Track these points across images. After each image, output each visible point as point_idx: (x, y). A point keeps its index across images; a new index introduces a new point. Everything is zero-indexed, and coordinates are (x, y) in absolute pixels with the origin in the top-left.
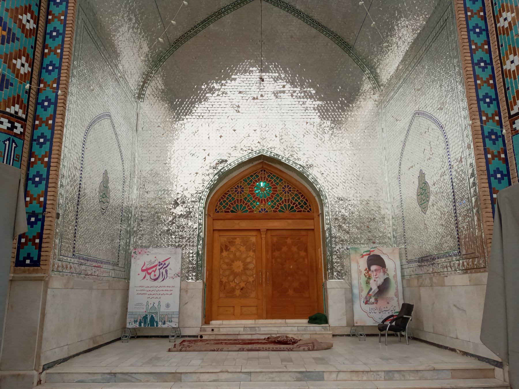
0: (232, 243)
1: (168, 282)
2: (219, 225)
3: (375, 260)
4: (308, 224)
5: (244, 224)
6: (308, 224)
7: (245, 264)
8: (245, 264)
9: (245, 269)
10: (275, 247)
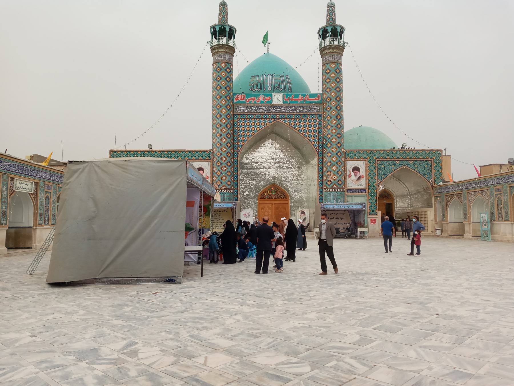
0: (265, 207)
1: (250, 218)
2: (261, 202)
3: (303, 213)
4: (286, 202)
5: (268, 202)
6: (286, 202)
7: (268, 213)
8: (268, 213)
9: (268, 214)
10: (277, 208)
